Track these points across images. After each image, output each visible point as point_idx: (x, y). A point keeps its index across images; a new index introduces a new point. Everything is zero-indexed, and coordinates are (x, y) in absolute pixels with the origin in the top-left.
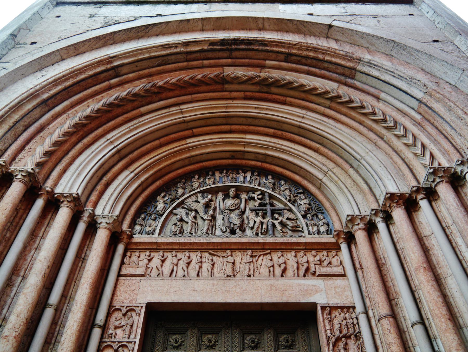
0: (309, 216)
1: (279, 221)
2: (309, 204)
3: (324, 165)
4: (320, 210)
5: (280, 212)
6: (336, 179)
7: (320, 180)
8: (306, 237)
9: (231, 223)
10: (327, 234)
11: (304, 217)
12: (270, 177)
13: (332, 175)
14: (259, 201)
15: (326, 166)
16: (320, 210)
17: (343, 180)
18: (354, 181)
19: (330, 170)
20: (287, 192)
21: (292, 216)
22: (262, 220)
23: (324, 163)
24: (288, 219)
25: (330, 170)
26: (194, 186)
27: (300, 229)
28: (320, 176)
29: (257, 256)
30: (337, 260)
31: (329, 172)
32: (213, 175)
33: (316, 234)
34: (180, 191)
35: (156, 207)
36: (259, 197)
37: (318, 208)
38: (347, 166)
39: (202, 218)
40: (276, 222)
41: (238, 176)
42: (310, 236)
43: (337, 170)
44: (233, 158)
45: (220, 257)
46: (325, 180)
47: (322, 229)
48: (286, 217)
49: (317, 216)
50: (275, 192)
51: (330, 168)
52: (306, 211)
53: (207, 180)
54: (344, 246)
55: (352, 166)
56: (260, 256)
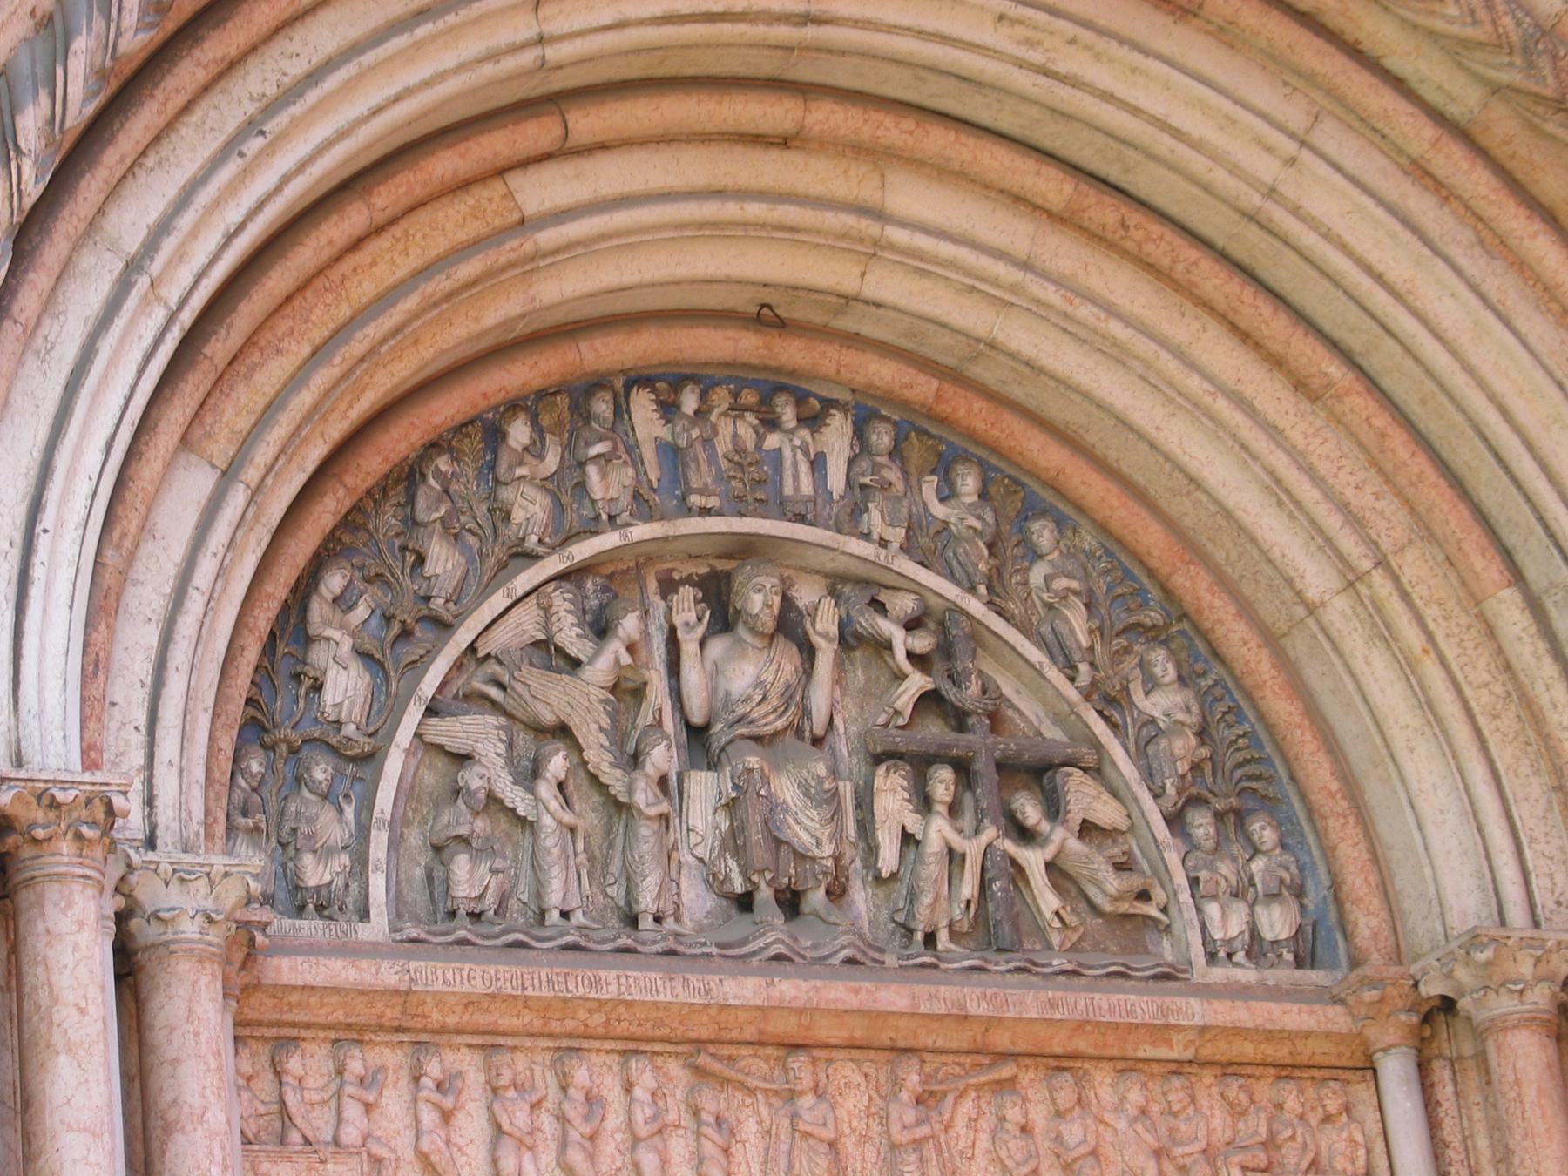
0: (1202, 824)
1: (1049, 852)
2: (1202, 734)
3: (1344, 508)
4: (1259, 778)
5: (1039, 773)
6: (1412, 636)
7: (1311, 609)
8: (1197, 978)
9: (779, 842)
10: (1299, 963)
11: (1175, 821)
12: (968, 484)
13: (1395, 607)
14: (917, 682)
15: (1355, 521)
16: (1259, 778)
17: (1450, 654)
18: (1508, 667)
19: (1381, 563)
20: (1077, 623)
21: (1107, 813)
22: (957, 842)
23: (1349, 494)
24: (1088, 830)
25: (1381, 563)
26: (518, 515)
27: (1153, 911)
28: (1317, 578)
29: (950, 1098)
30: (1352, 1142)
31: (1378, 577)
32: (621, 410)
33: (1240, 957)
34: (443, 560)
35: (318, 687)
36: (922, 642)
37: (1247, 761)
38: (1487, 568)
39: (602, 788)
40: (1033, 859)
41: (772, 441)
42: (1218, 974)
43: (1415, 566)
44: (765, 319)
45: (752, 1092)
46: (1338, 612)
47: (1277, 923)
48: (1076, 818)
49: (1240, 816)
50: (1000, 613)
51: (1386, 545)
52: (1183, 777)
53: (592, 471)
54: (1396, 1070)
55: (1516, 575)
56: (962, 1095)
